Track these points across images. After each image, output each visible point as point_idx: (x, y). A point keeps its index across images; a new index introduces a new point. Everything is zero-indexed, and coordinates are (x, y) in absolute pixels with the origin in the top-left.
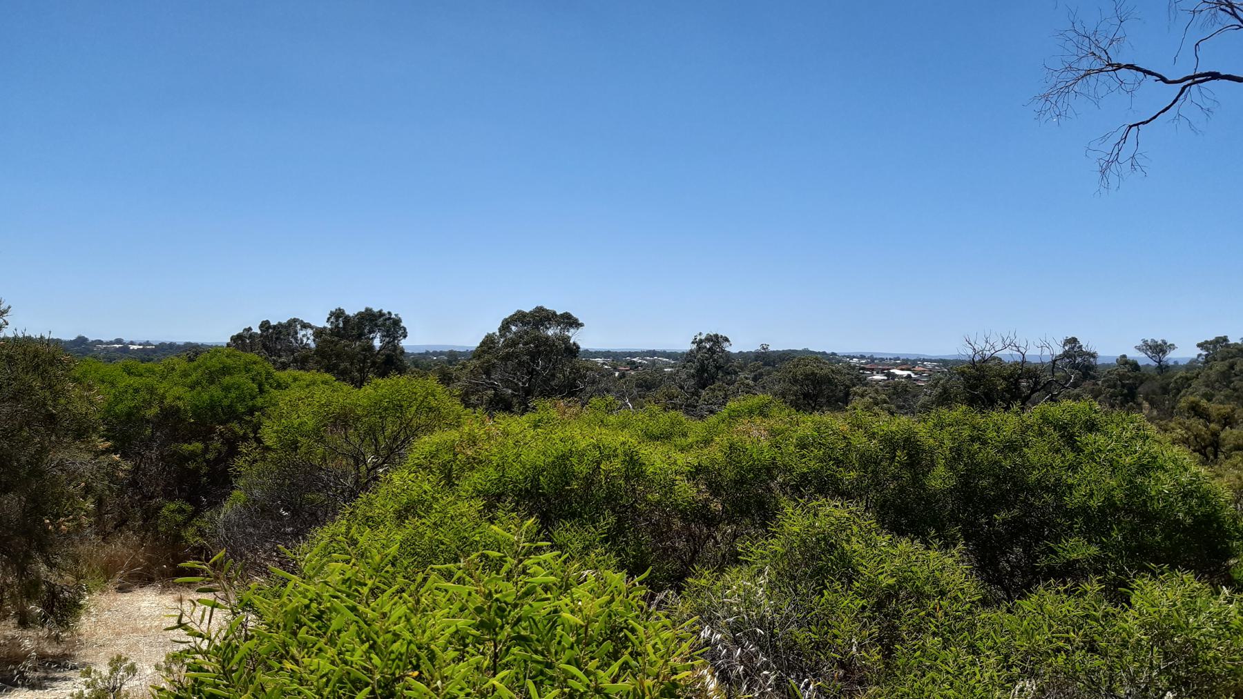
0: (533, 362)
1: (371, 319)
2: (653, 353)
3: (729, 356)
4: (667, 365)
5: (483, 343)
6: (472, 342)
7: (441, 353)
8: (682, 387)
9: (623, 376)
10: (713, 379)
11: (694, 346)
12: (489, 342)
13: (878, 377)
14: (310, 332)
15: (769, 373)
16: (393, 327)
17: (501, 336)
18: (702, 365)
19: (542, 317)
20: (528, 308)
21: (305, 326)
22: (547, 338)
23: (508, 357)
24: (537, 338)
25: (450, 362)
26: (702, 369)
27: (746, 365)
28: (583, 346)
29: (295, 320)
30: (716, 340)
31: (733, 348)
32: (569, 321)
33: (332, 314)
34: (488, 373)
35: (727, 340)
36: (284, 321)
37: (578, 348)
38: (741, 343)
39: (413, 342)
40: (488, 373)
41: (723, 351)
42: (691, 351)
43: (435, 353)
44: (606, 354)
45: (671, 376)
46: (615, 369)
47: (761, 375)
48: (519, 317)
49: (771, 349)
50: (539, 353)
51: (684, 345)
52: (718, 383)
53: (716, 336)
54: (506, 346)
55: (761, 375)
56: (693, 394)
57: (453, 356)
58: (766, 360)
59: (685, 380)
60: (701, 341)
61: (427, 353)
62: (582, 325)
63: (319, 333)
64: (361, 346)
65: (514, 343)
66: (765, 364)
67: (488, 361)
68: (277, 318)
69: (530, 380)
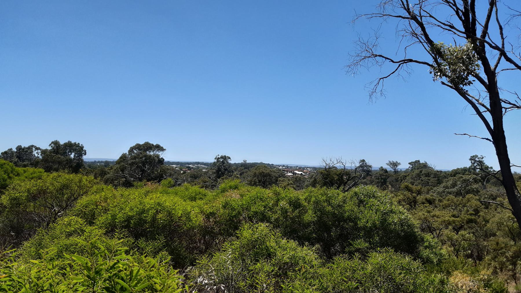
0: (143, 165)
1: (70, 146)
2: (198, 163)
3: (230, 165)
4: (204, 168)
5: (121, 158)
6: (115, 156)
7: (102, 162)
8: (210, 178)
9: (184, 173)
10: (223, 174)
11: (216, 160)
12: (123, 158)
13: (290, 174)
14: (39, 151)
15: (247, 172)
16: (80, 150)
17: (129, 155)
18: (219, 168)
19: (148, 147)
20: (142, 143)
21: (37, 149)
22: (150, 156)
23: (132, 164)
24: (146, 156)
25: (106, 166)
26: (219, 170)
27: (237, 169)
28: (166, 160)
29: (32, 146)
30: (225, 158)
31: (232, 162)
32: (159, 148)
33: (52, 143)
34: (122, 171)
35: (230, 158)
36: (27, 146)
37: (164, 160)
38: (235, 159)
39: (89, 157)
40: (122, 171)
41: (228, 163)
42: (214, 162)
43: (99, 162)
44: (177, 163)
45: (206, 173)
46: (181, 170)
47: (243, 173)
48: (138, 147)
49: (248, 162)
50: (147, 162)
51: (211, 160)
52: (225, 176)
53: (225, 156)
54: (132, 159)
55: (243, 173)
56: (215, 181)
57: (107, 163)
58: (245, 167)
59: (211, 175)
60: (219, 158)
61: (95, 162)
62: (165, 150)
63: (44, 152)
64: (64, 157)
65: (135, 158)
66: (245, 168)
67: (123, 165)
68: (25, 144)
69: (142, 174)
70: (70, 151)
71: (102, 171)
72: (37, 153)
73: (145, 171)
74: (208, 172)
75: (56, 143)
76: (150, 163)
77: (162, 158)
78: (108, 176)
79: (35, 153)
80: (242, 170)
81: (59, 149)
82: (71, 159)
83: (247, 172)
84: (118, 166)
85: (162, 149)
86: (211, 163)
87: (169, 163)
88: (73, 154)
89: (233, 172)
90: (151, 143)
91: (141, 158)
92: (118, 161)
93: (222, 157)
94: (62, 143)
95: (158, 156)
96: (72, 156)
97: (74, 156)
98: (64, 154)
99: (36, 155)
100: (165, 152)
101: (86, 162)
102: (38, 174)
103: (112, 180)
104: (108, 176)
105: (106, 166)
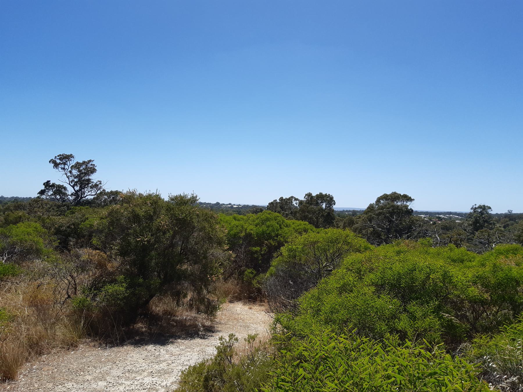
0: (392, 219)
1: (321, 197)
2: (450, 213)
3: (491, 216)
4: (457, 219)
5: (369, 208)
6: (364, 206)
7: (350, 211)
8: (465, 230)
9: (434, 223)
10: (482, 227)
11: (472, 211)
12: (371, 208)
14: (298, 202)
15: (512, 224)
16: (330, 200)
17: (376, 205)
18: (476, 220)
19: (395, 197)
20: (389, 193)
21: (296, 199)
22: (398, 206)
23: (380, 214)
24: (393, 206)
25: (353, 215)
26: (476, 222)
27: (500, 220)
28: (414, 209)
29: (292, 197)
30: (484, 208)
31: (493, 212)
32: (408, 199)
33: (306, 195)
34: (370, 221)
35: (490, 208)
36: (288, 197)
37: (412, 211)
38: (498, 208)
40: (370, 221)
41: (488, 213)
42: (471, 213)
43: (347, 211)
44: (426, 213)
45: (460, 225)
46: (431, 220)
47: (508, 225)
48: (385, 197)
49: (513, 212)
50: (394, 213)
51: (467, 209)
52: (484, 229)
53: (484, 206)
54: (379, 209)
55: (508, 225)
56: (471, 233)
57: (354, 213)
58: (511, 219)
59: (467, 227)
60: (476, 208)
61: (344, 211)
62: (413, 200)
63: (301, 202)
65: (382, 208)
66: (510, 220)
67: (371, 216)
68: (286, 196)
69: (389, 225)
70: (322, 202)
71: (350, 219)
72: (296, 203)
73: (393, 222)
74: (463, 224)
75: (309, 195)
76: (398, 213)
77: (411, 209)
78: (356, 226)
79: (294, 203)
80: (507, 221)
81: (312, 201)
82: (322, 209)
83: (512, 224)
84: (365, 216)
85: (409, 199)
86: (466, 214)
87: (418, 213)
88: (324, 204)
89: (494, 224)
90: (398, 192)
91: (388, 208)
92: (365, 211)
93: (480, 207)
94: (314, 194)
95: (406, 207)
96: (324, 206)
97: (326, 206)
98: (317, 204)
99: (295, 205)
100: (413, 202)
101: (336, 211)
102: (303, 226)
103: (361, 230)
104: (356, 226)
105: (353, 215)
